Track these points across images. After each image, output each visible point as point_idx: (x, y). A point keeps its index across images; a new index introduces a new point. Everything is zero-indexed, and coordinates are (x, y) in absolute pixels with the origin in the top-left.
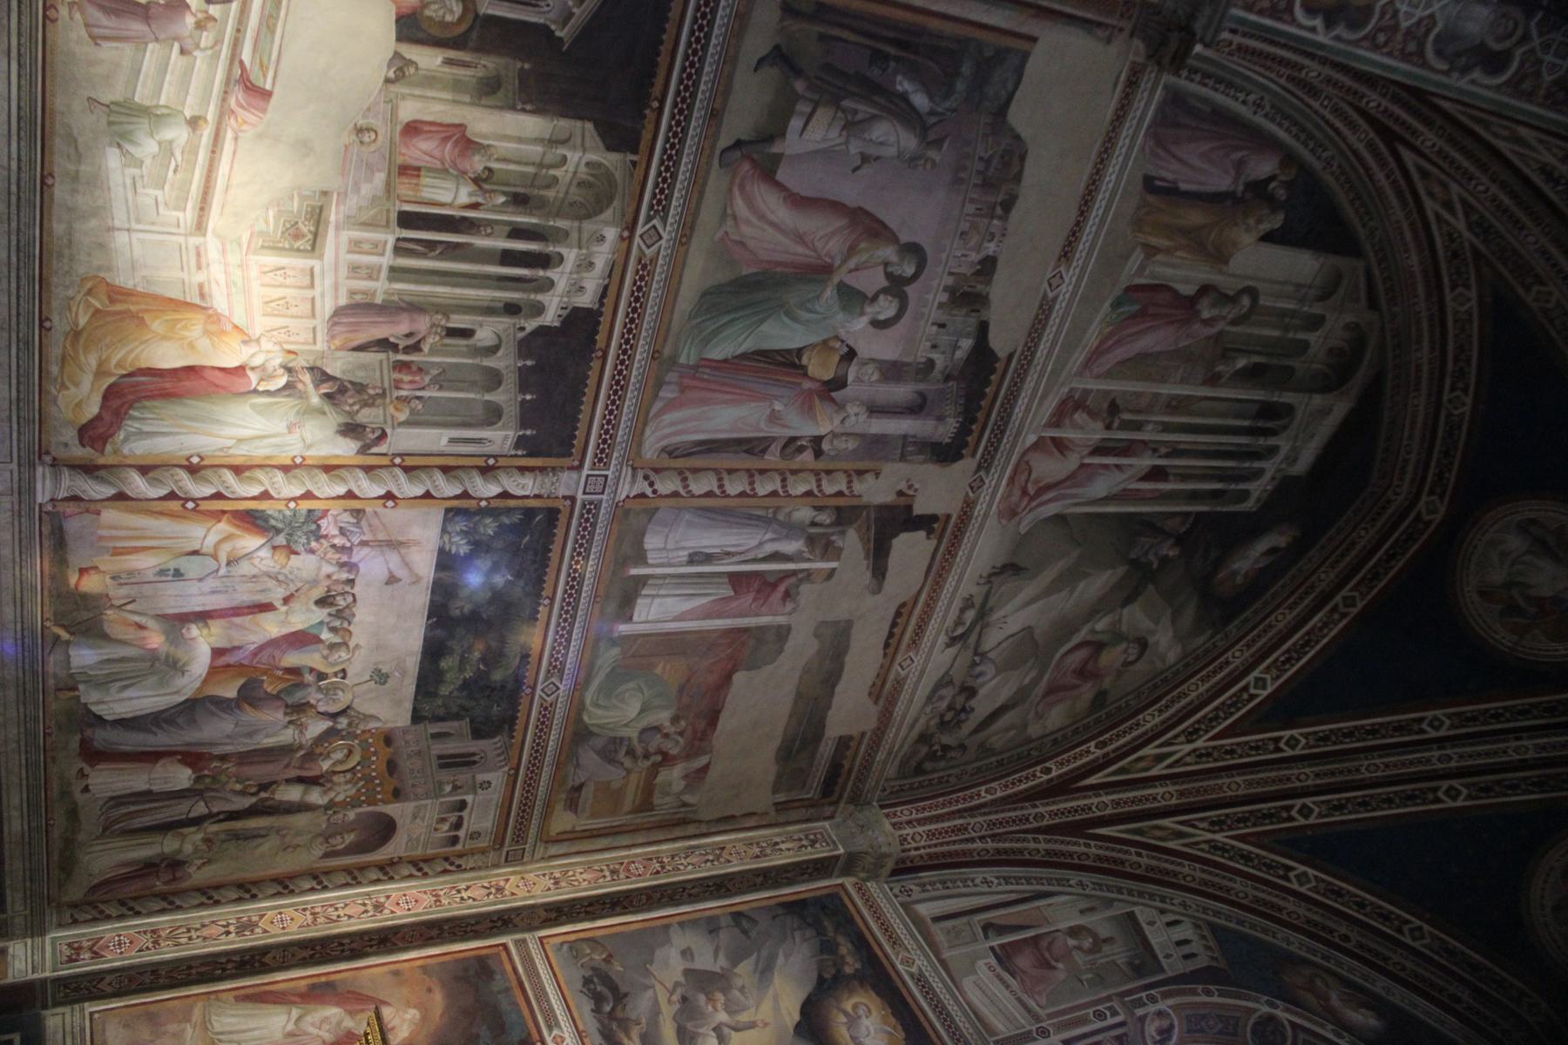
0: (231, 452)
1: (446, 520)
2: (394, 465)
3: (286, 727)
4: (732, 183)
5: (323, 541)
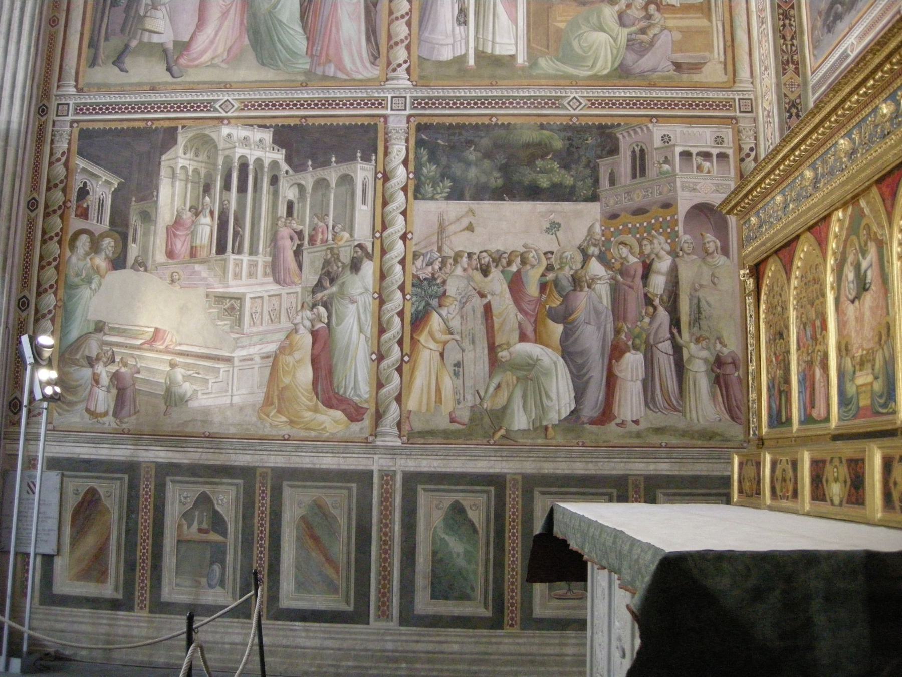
0: (369, 335)
1: (424, 199)
2: (381, 236)
3: (594, 289)
4: (191, 67)
5: (436, 276)
